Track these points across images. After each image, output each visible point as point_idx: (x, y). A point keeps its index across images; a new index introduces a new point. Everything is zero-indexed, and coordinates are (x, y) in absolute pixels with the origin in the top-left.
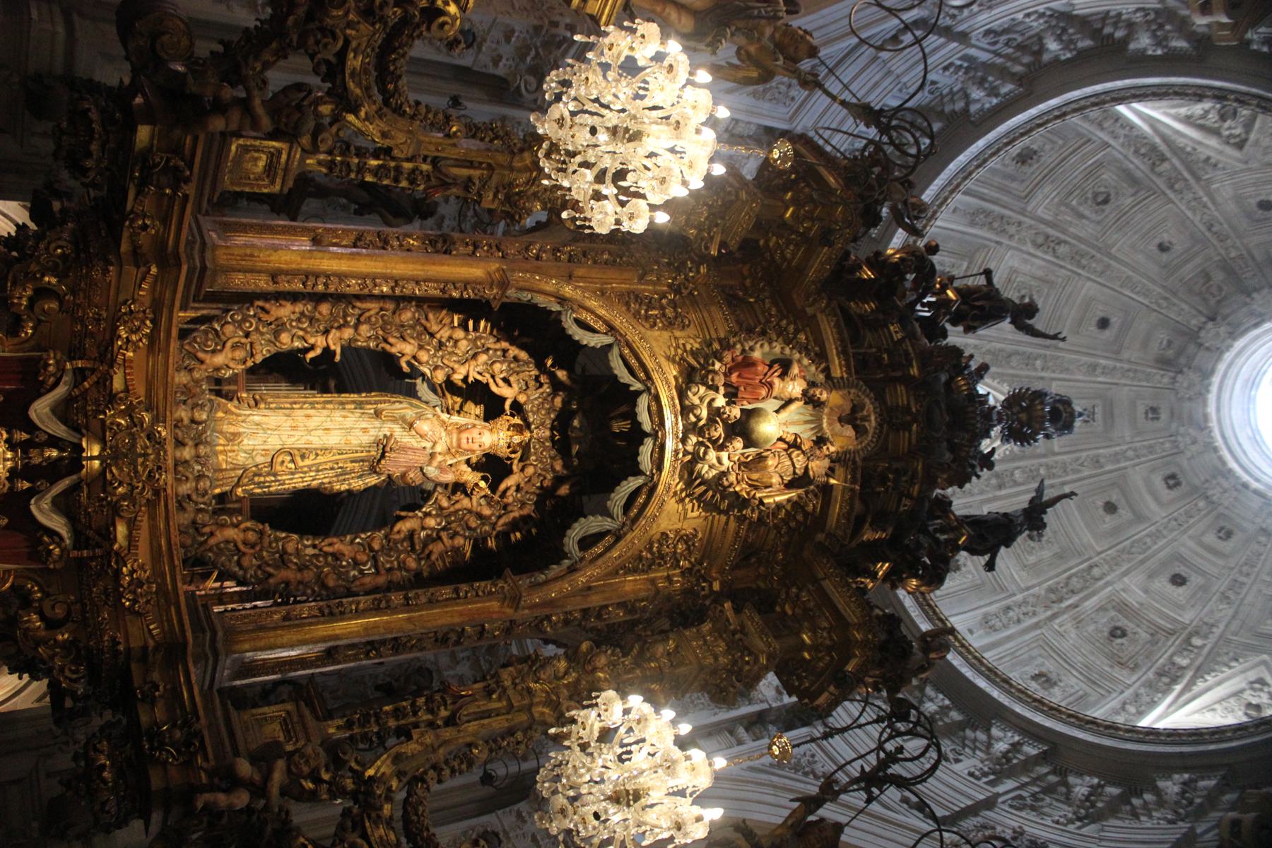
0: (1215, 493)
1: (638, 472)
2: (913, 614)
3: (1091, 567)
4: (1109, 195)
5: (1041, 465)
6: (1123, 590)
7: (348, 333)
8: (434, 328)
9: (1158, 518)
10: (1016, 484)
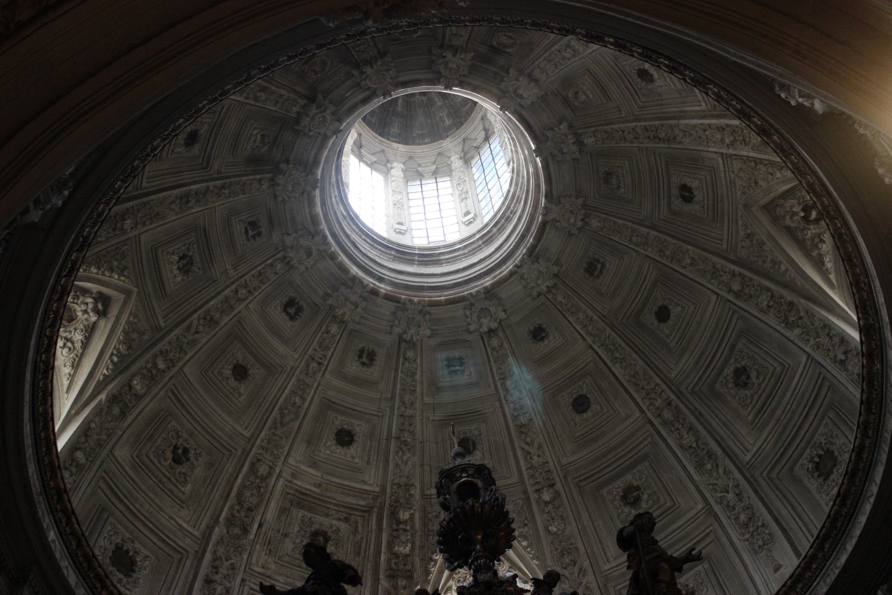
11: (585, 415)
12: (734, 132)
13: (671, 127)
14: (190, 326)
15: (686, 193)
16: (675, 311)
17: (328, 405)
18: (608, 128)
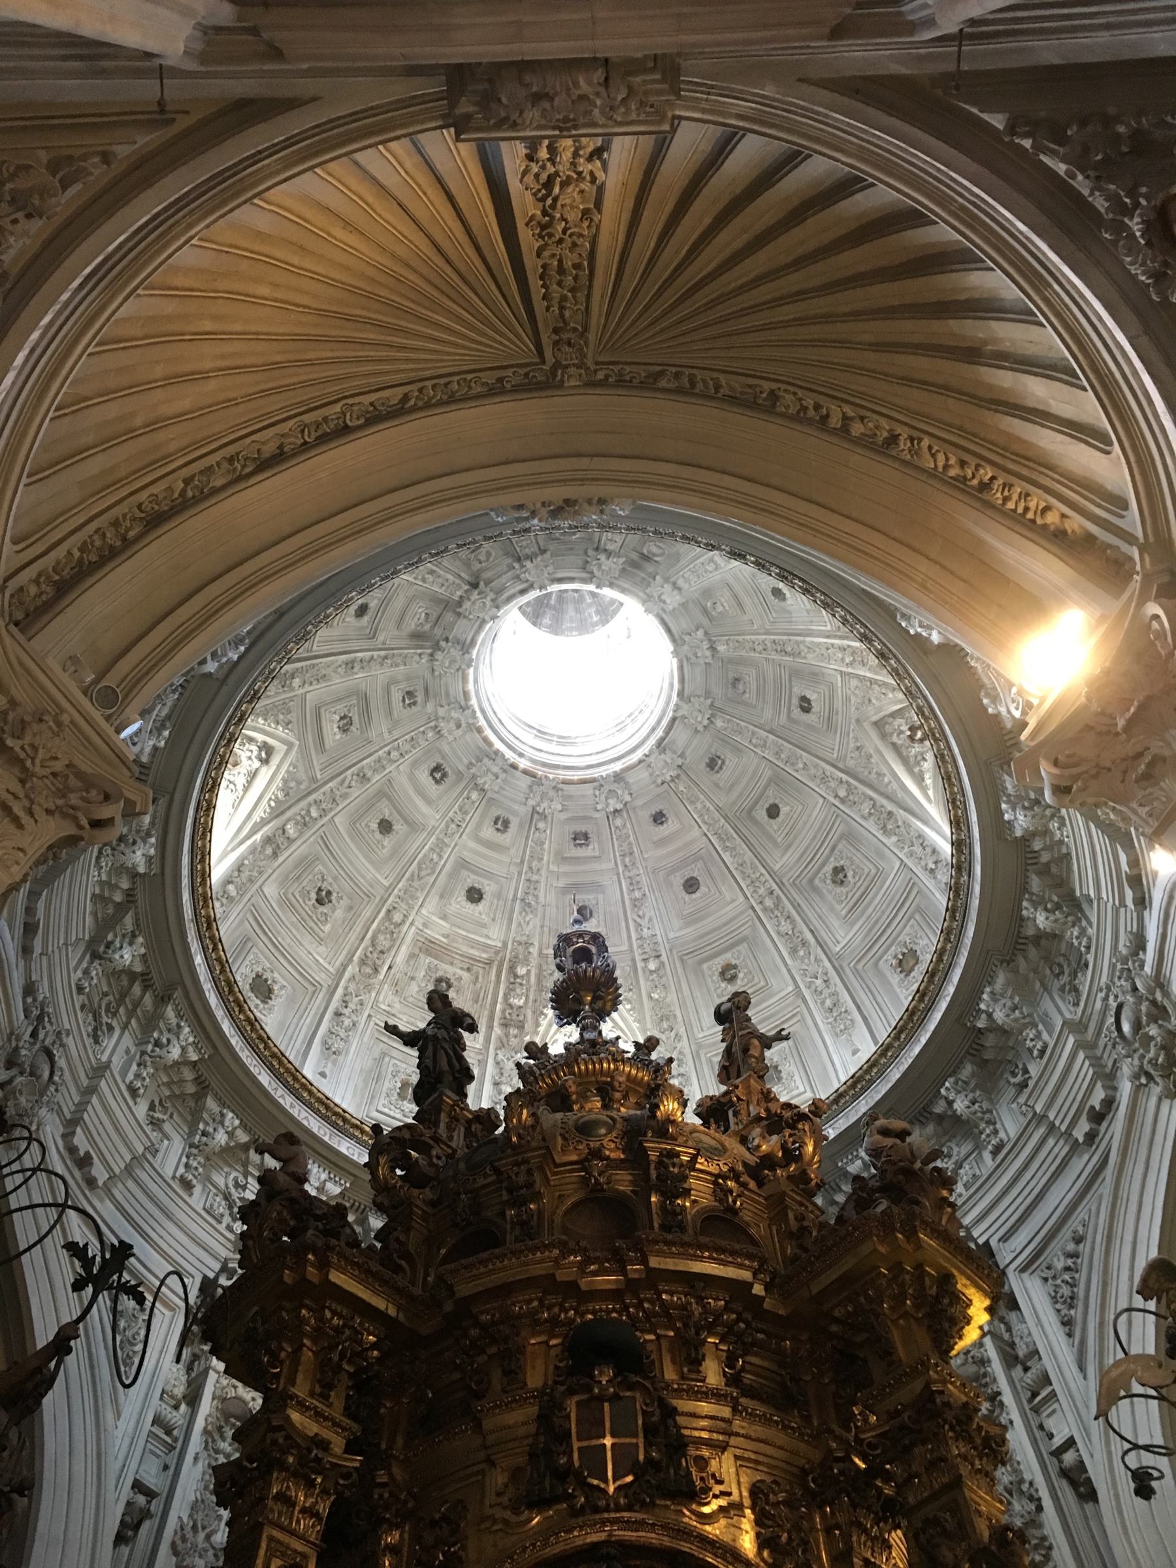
0: (486, 781)
9: (432, 823)
11: (694, 896)
12: (853, 653)
13: (797, 643)
14: (344, 781)
15: (805, 705)
16: (784, 810)
17: (463, 864)
18: (740, 638)
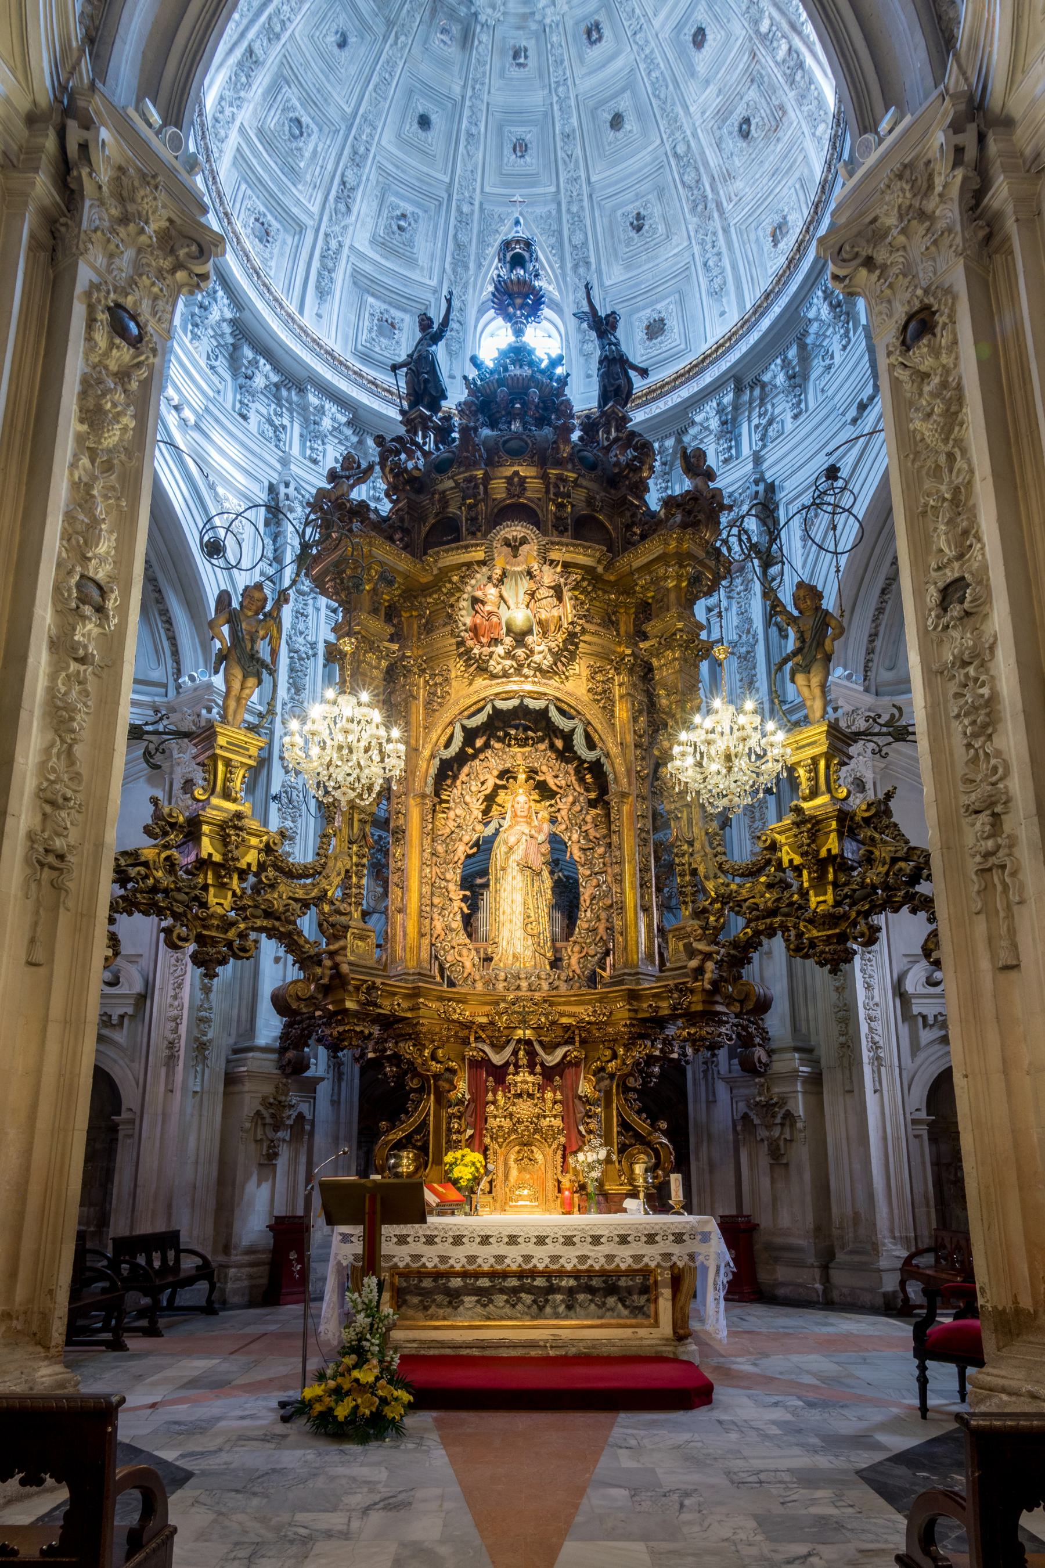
1: (546, 710)
2: (696, 389)
3: (676, 155)
4: (291, 120)
5: (568, 210)
6: (703, 113)
7: (452, 887)
8: (447, 831)
10: (585, 243)
